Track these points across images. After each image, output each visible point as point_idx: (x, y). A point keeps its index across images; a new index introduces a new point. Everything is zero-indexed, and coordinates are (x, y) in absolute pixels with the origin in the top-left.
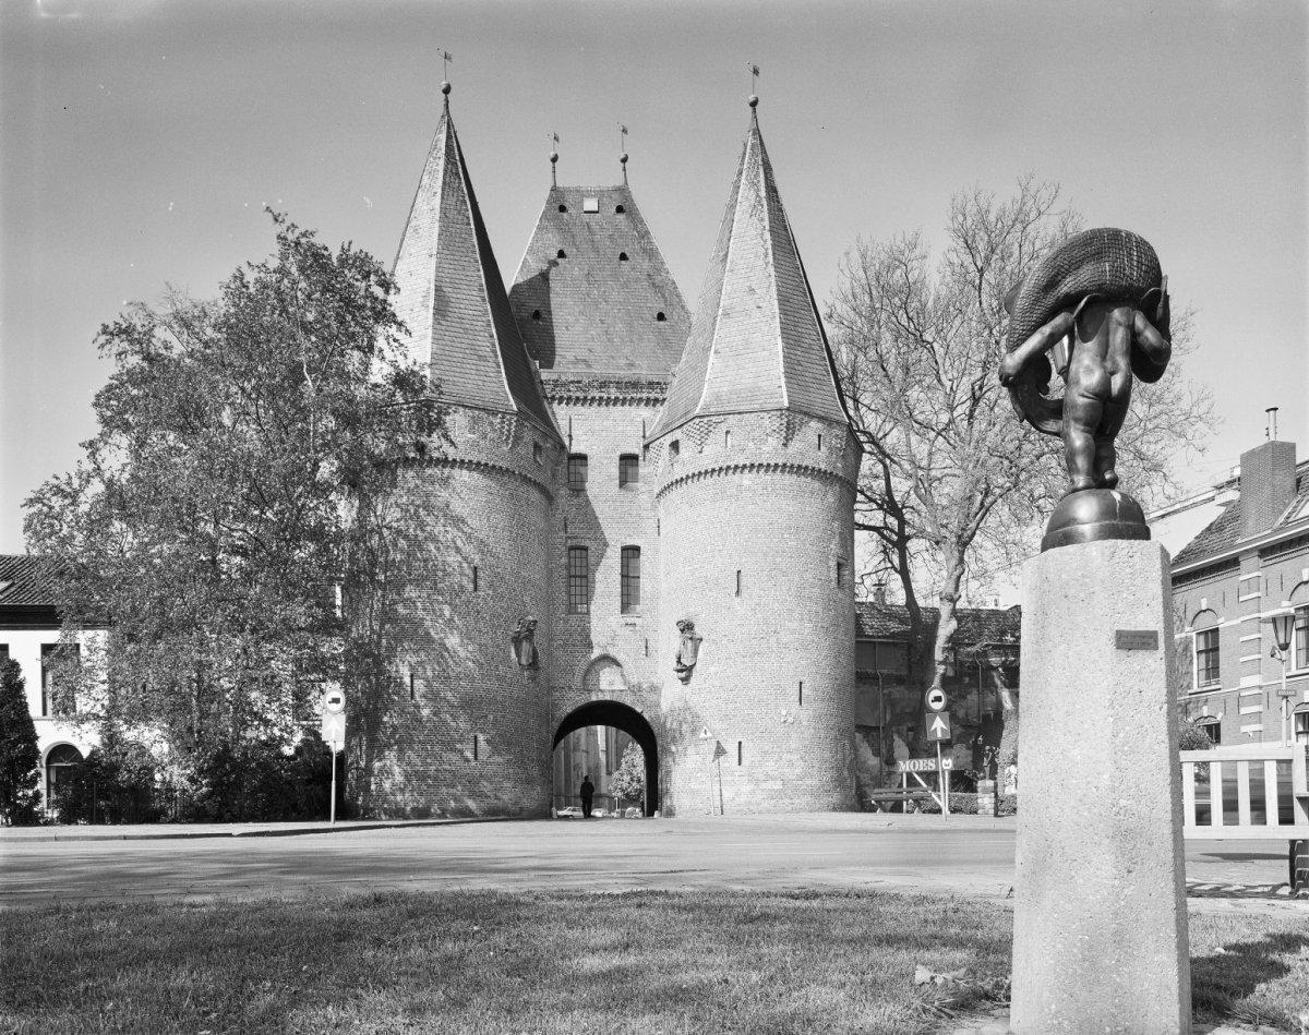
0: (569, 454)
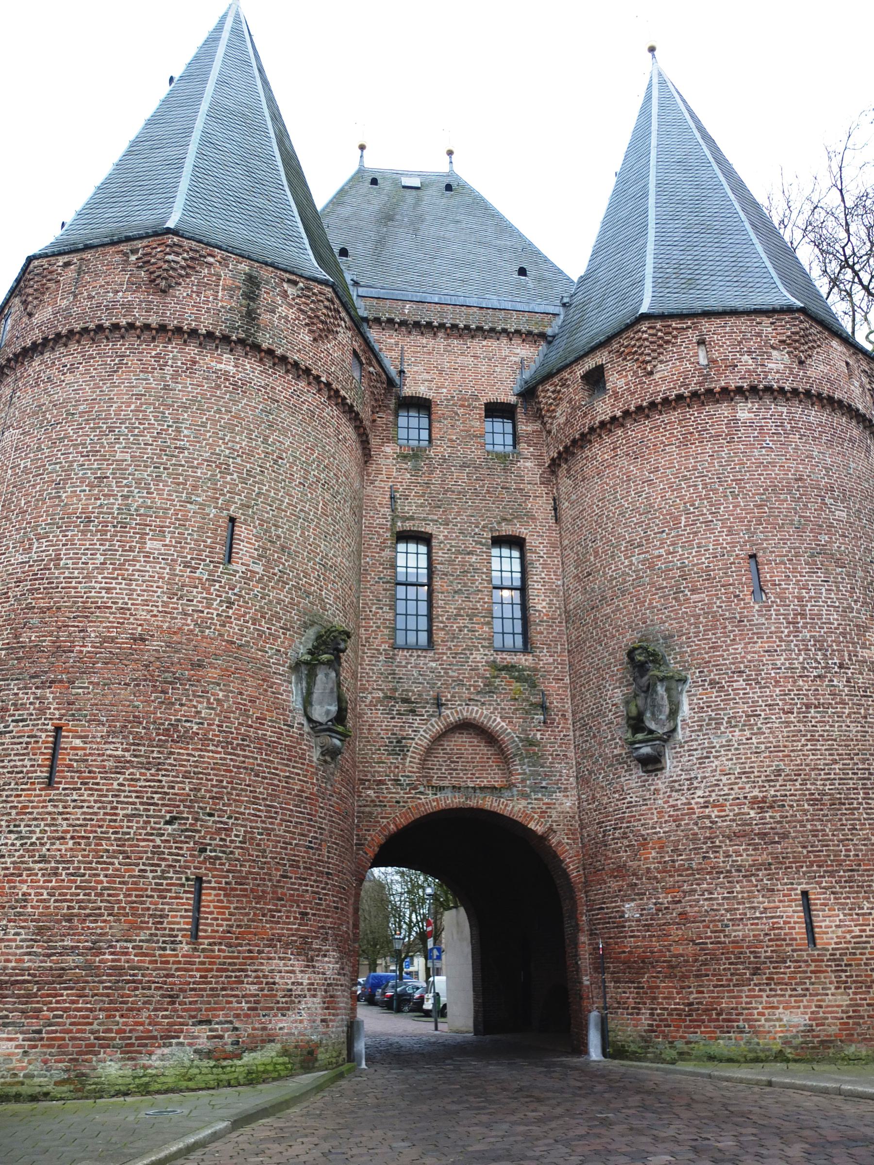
0: (398, 397)
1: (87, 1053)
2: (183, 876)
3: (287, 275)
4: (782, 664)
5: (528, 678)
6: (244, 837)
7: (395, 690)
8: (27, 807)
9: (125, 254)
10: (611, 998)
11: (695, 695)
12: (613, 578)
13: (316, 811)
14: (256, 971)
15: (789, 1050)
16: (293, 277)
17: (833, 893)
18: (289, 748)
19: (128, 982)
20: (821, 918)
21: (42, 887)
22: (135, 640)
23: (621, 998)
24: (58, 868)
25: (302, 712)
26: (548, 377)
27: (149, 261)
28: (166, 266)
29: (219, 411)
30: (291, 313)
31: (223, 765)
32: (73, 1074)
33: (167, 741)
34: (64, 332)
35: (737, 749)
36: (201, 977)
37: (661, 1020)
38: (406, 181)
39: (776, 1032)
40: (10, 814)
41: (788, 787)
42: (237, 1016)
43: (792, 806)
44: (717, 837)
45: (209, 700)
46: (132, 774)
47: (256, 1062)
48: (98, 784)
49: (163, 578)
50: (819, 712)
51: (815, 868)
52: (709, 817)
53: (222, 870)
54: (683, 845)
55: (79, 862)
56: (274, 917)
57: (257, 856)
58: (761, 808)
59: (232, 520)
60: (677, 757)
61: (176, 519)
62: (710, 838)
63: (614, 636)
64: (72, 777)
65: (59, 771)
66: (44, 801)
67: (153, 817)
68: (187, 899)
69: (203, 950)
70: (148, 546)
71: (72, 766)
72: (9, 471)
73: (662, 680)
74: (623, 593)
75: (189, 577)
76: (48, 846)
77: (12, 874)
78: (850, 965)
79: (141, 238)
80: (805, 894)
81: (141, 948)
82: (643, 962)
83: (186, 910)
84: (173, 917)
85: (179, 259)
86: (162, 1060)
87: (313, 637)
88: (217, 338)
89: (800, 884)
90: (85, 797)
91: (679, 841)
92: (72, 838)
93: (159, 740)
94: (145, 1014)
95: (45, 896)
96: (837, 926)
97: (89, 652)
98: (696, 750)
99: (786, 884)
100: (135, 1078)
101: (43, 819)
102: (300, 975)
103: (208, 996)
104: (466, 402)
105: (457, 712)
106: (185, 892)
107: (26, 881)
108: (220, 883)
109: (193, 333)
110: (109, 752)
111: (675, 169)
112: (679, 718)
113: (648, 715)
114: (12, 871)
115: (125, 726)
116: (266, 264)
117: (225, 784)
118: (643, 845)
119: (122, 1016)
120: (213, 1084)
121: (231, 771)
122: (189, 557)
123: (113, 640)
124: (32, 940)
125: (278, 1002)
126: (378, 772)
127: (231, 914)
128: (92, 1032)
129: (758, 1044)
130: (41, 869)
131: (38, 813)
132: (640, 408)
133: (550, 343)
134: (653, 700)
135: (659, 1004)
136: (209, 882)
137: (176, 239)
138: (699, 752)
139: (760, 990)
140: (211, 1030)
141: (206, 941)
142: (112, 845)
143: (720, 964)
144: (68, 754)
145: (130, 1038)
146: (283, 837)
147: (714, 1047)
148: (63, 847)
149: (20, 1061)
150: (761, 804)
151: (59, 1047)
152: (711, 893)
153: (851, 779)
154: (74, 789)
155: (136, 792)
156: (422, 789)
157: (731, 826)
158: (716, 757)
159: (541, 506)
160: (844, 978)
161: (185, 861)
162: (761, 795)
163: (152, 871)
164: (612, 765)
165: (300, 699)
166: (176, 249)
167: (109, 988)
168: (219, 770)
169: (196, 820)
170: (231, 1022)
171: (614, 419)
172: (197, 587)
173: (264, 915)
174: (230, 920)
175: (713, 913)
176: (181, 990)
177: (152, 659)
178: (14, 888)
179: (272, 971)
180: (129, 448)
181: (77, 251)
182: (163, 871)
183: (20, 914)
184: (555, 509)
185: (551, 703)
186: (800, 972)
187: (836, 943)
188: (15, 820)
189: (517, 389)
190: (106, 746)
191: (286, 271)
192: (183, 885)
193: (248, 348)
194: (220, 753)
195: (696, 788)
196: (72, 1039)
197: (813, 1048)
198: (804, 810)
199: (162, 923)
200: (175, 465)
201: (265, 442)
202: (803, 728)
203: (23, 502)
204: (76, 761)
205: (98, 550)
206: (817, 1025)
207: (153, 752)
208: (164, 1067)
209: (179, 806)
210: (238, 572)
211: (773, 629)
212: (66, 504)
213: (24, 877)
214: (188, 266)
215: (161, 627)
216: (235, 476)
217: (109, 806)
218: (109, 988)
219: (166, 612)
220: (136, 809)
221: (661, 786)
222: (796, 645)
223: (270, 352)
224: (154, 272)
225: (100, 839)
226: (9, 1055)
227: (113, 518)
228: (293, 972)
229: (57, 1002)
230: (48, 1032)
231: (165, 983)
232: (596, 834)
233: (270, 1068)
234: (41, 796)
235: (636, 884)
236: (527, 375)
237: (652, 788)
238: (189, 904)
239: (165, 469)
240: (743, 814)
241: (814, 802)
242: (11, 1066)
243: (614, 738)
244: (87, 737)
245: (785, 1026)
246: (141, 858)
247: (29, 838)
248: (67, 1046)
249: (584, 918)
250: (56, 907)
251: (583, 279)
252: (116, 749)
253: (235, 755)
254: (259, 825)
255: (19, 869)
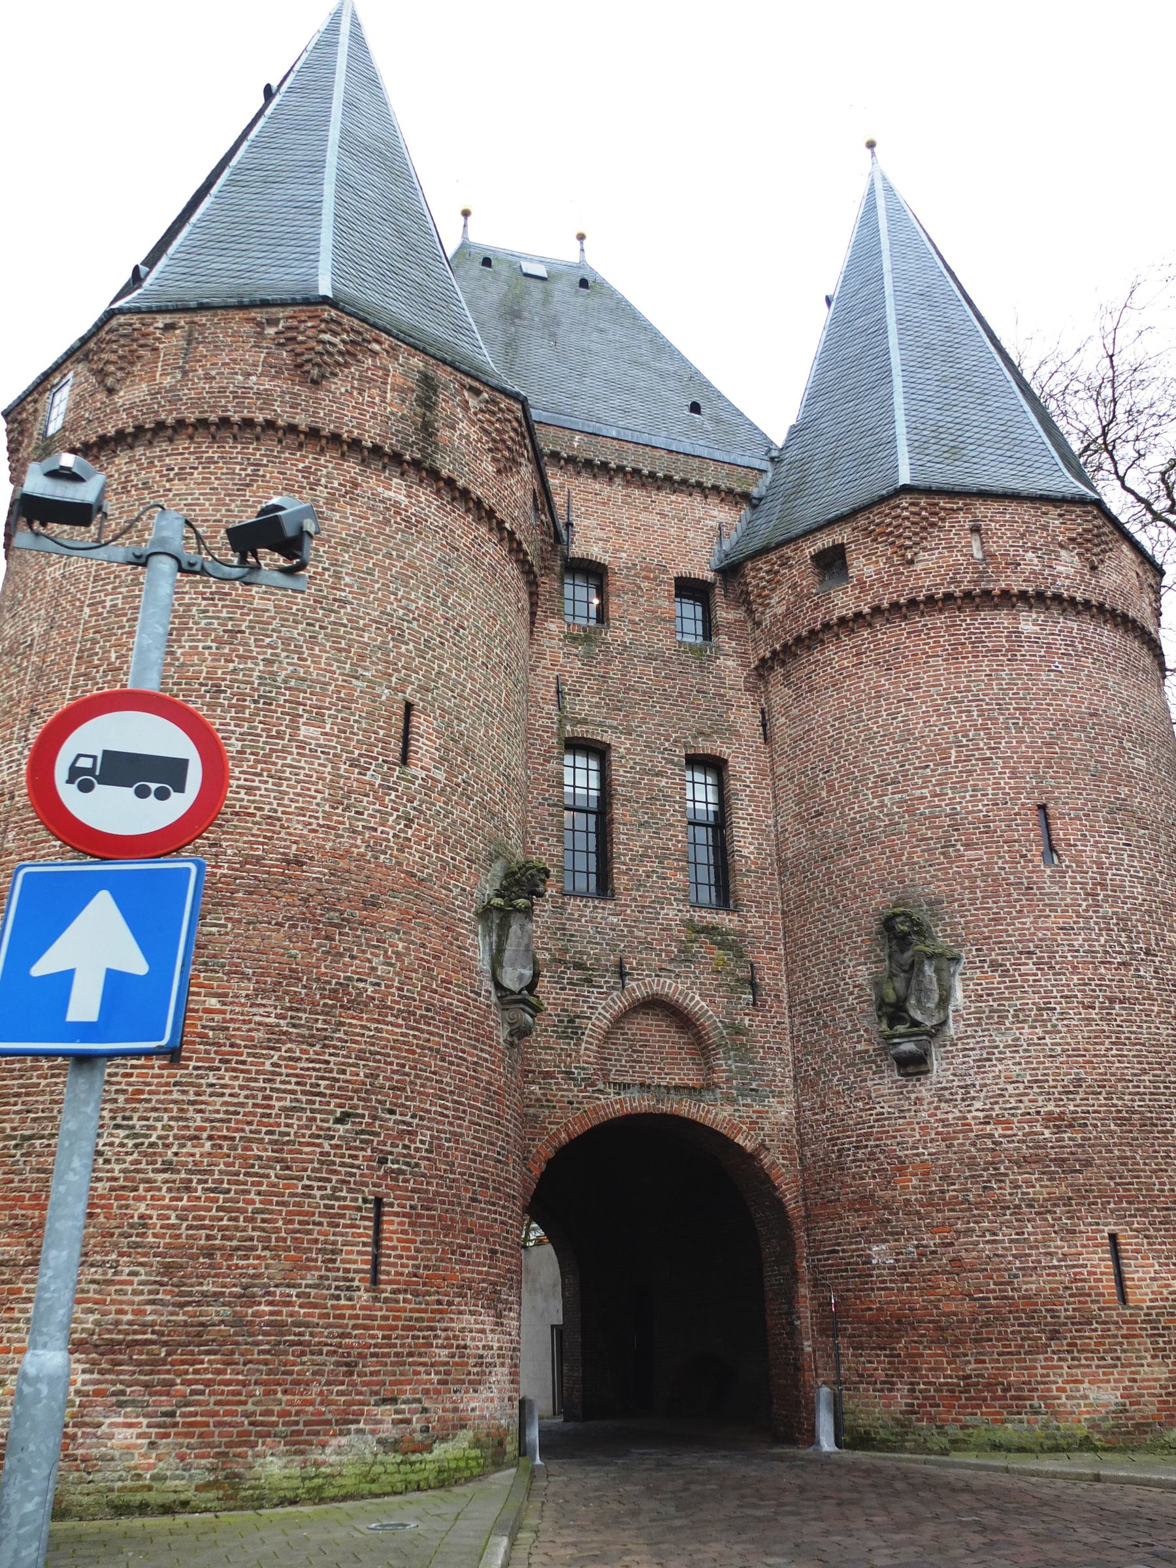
1: (239, 1445)
2: (360, 1196)
3: (469, 380)
4: (1081, 946)
5: (732, 944)
6: (431, 1143)
7: (566, 951)
8: (142, 1092)
9: (259, 324)
10: (849, 1369)
11: (971, 979)
12: (855, 822)
13: (504, 1111)
14: (445, 1330)
15: (1097, 1436)
16: (476, 384)
17: (1146, 1237)
18: (477, 1024)
19: (292, 1344)
20: (1133, 1268)
21: (168, 1208)
22: (288, 862)
23: (865, 1369)
24: (191, 1181)
25: (489, 975)
26: (764, 551)
27: (294, 339)
28: (319, 348)
29: (388, 555)
30: (474, 433)
31: (404, 1043)
32: (221, 1475)
33: (334, 1007)
34: (170, 421)
35: (1026, 1051)
36: (384, 1337)
37: (925, 1398)
38: (528, 268)
39: (1081, 1413)
40: (115, 1101)
41: (1091, 1102)
42: (426, 1392)
43: (1095, 1126)
44: (1002, 1162)
45: (386, 952)
46: (289, 1050)
47: (449, 1456)
48: (244, 1063)
49: (324, 779)
50: (1124, 1009)
51: (1125, 1205)
52: (991, 1136)
53: (406, 1189)
54: (956, 1171)
55: (221, 1172)
56: (463, 1255)
57: (445, 1171)
58: (1058, 1127)
59: (409, 707)
60: (948, 1057)
61: (339, 699)
62: (992, 1163)
63: (857, 897)
64: (207, 1052)
65: (188, 1043)
66: (167, 1084)
67: (320, 1112)
68: (365, 1228)
69: (386, 1300)
70: (302, 732)
71: (206, 1036)
72: (87, 610)
73: (931, 957)
74: (871, 842)
75: (357, 780)
76: (175, 1149)
77: (123, 1188)
78: (1169, 1328)
79: (283, 304)
80: (1113, 1237)
81: (308, 1295)
82: (899, 1322)
83: (365, 1244)
84: (348, 1252)
85: (336, 340)
86: (344, 1454)
87: (501, 874)
88: (386, 454)
89: (1106, 1225)
90: (227, 1081)
91: (950, 1165)
92: (210, 1138)
93: (325, 1005)
94: (315, 1389)
95: (173, 1221)
96: (1152, 1279)
97: (225, 876)
98: (973, 1049)
99: (1090, 1224)
100: (304, 1479)
101: (166, 1110)
102: (490, 1336)
103: (393, 1364)
104: (652, 572)
105: (645, 985)
106: (363, 1218)
107: (144, 1198)
108: (404, 1207)
109: (355, 444)
110: (257, 1018)
111: (893, 303)
112: (951, 1008)
113: (913, 1002)
114: (121, 1183)
115: (279, 982)
116: (444, 362)
117: (407, 1069)
118: (898, 1170)
119: (285, 1392)
120: (400, 1487)
121: (414, 1053)
122: (357, 752)
123: (259, 859)
124: (155, 1282)
125: (469, 1373)
126: (545, 1061)
127: (417, 1250)
128: (246, 1415)
129: (1058, 1428)
130: (167, 1182)
131: (158, 1101)
132: (895, 606)
133: (754, 507)
134: (920, 982)
135: (921, 1377)
136: (391, 1205)
137: (333, 313)
138: (978, 1052)
139: (1060, 1359)
140: (397, 1412)
141: (389, 1288)
142: (266, 1150)
143: (1007, 1326)
144: (200, 1019)
145: (297, 1423)
146: (472, 1145)
147: (999, 1433)
148: (197, 1151)
149: (145, 1456)
150: (1057, 1122)
151: (201, 1435)
152: (995, 1234)
153: (1163, 1094)
154: (210, 1069)
155: (297, 1076)
156: (601, 1086)
157: (1020, 1148)
158: (1000, 1060)
159: (746, 719)
160: (1162, 1345)
161: (361, 1175)
162: (1058, 1110)
163: (319, 1188)
164: (853, 1065)
165: (487, 958)
166: (333, 327)
167: (268, 1352)
168: (400, 1049)
169: (374, 1118)
170: (419, 1401)
171: (859, 615)
172: (367, 795)
173: (453, 1253)
174: (416, 1258)
175: (996, 1259)
176: (360, 1355)
177: (312, 891)
178: (127, 1207)
179: (462, 1330)
180: (273, 594)
181: (186, 310)
182: (334, 1189)
183: (138, 1245)
184: (764, 725)
185: (762, 979)
186: (1109, 1337)
187: (1152, 1300)
188: (124, 1110)
189: (715, 563)
190: (254, 1010)
191: (467, 374)
192: (359, 1209)
193: (424, 474)
194: (400, 1026)
195: (974, 1098)
196: (218, 1424)
197: (1129, 1433)
198: (1111, 1131)
199: (334, 1261)
200: (335, 623)
201: (444, 603)
202: (1106, 1028)
203: (113, 655)
204: (213, 1029)
205: (233, 732)
206: (1131, 1404)
207: (317, 1020)
208: (341, 1464)
209: (352, 1099)
210: (416, 777)
211: (1069, 901)
212: (183, 665)
213: (141, 1192)
214: (348, 352)
215: (323, 847)
216: (411, 647)
217: (260, 1094)
218: (268, 1352)
219: (328, 827)
220: (297, 1100)
221: (924, 1094)
222: (1096, 923)
223: (450, 482)
224: (302, 354)
225: (250, 1140)
226: (128, 1447)
227: (253, 689)
228: (483, 1331)
229: (196, 1372)
230: (183, 1415)
231: (340, 1345)
232: (826, 1154)
233: (462, 1464)
234: (161, 1076)
235: (888, 1221)
236: (726, 546)
237: (913, 1096)
238: (367, 1236)
239: (321, 627)
240: (1036, 1134)
241: (1121, 1121)
242: (132, 1463)
243: (861, 1030)
244: (226, 995)
245: (1091, 1405)
246: (305, 1170)
247: (147, 1136)
248: (212, 1434)
249: (804, 1264)
250: (189, 1237)
251: (795, 432)
252: (268, 1014)
253: (418, 1030)
254: (446, 1127)
255: (133, 1180)
